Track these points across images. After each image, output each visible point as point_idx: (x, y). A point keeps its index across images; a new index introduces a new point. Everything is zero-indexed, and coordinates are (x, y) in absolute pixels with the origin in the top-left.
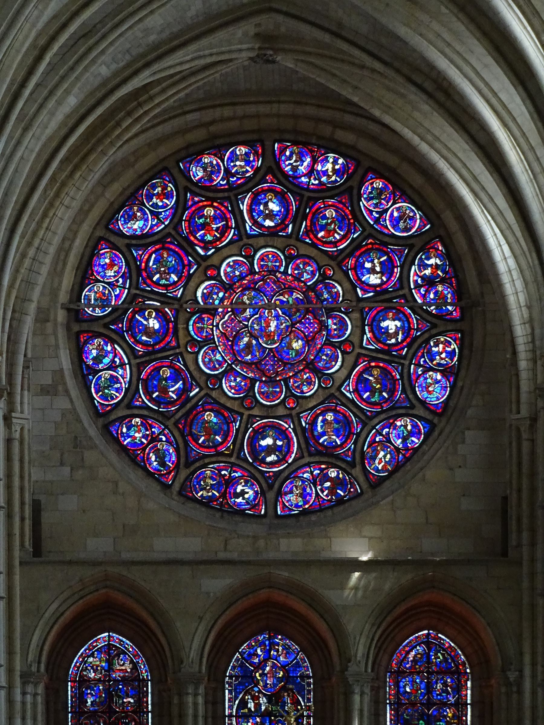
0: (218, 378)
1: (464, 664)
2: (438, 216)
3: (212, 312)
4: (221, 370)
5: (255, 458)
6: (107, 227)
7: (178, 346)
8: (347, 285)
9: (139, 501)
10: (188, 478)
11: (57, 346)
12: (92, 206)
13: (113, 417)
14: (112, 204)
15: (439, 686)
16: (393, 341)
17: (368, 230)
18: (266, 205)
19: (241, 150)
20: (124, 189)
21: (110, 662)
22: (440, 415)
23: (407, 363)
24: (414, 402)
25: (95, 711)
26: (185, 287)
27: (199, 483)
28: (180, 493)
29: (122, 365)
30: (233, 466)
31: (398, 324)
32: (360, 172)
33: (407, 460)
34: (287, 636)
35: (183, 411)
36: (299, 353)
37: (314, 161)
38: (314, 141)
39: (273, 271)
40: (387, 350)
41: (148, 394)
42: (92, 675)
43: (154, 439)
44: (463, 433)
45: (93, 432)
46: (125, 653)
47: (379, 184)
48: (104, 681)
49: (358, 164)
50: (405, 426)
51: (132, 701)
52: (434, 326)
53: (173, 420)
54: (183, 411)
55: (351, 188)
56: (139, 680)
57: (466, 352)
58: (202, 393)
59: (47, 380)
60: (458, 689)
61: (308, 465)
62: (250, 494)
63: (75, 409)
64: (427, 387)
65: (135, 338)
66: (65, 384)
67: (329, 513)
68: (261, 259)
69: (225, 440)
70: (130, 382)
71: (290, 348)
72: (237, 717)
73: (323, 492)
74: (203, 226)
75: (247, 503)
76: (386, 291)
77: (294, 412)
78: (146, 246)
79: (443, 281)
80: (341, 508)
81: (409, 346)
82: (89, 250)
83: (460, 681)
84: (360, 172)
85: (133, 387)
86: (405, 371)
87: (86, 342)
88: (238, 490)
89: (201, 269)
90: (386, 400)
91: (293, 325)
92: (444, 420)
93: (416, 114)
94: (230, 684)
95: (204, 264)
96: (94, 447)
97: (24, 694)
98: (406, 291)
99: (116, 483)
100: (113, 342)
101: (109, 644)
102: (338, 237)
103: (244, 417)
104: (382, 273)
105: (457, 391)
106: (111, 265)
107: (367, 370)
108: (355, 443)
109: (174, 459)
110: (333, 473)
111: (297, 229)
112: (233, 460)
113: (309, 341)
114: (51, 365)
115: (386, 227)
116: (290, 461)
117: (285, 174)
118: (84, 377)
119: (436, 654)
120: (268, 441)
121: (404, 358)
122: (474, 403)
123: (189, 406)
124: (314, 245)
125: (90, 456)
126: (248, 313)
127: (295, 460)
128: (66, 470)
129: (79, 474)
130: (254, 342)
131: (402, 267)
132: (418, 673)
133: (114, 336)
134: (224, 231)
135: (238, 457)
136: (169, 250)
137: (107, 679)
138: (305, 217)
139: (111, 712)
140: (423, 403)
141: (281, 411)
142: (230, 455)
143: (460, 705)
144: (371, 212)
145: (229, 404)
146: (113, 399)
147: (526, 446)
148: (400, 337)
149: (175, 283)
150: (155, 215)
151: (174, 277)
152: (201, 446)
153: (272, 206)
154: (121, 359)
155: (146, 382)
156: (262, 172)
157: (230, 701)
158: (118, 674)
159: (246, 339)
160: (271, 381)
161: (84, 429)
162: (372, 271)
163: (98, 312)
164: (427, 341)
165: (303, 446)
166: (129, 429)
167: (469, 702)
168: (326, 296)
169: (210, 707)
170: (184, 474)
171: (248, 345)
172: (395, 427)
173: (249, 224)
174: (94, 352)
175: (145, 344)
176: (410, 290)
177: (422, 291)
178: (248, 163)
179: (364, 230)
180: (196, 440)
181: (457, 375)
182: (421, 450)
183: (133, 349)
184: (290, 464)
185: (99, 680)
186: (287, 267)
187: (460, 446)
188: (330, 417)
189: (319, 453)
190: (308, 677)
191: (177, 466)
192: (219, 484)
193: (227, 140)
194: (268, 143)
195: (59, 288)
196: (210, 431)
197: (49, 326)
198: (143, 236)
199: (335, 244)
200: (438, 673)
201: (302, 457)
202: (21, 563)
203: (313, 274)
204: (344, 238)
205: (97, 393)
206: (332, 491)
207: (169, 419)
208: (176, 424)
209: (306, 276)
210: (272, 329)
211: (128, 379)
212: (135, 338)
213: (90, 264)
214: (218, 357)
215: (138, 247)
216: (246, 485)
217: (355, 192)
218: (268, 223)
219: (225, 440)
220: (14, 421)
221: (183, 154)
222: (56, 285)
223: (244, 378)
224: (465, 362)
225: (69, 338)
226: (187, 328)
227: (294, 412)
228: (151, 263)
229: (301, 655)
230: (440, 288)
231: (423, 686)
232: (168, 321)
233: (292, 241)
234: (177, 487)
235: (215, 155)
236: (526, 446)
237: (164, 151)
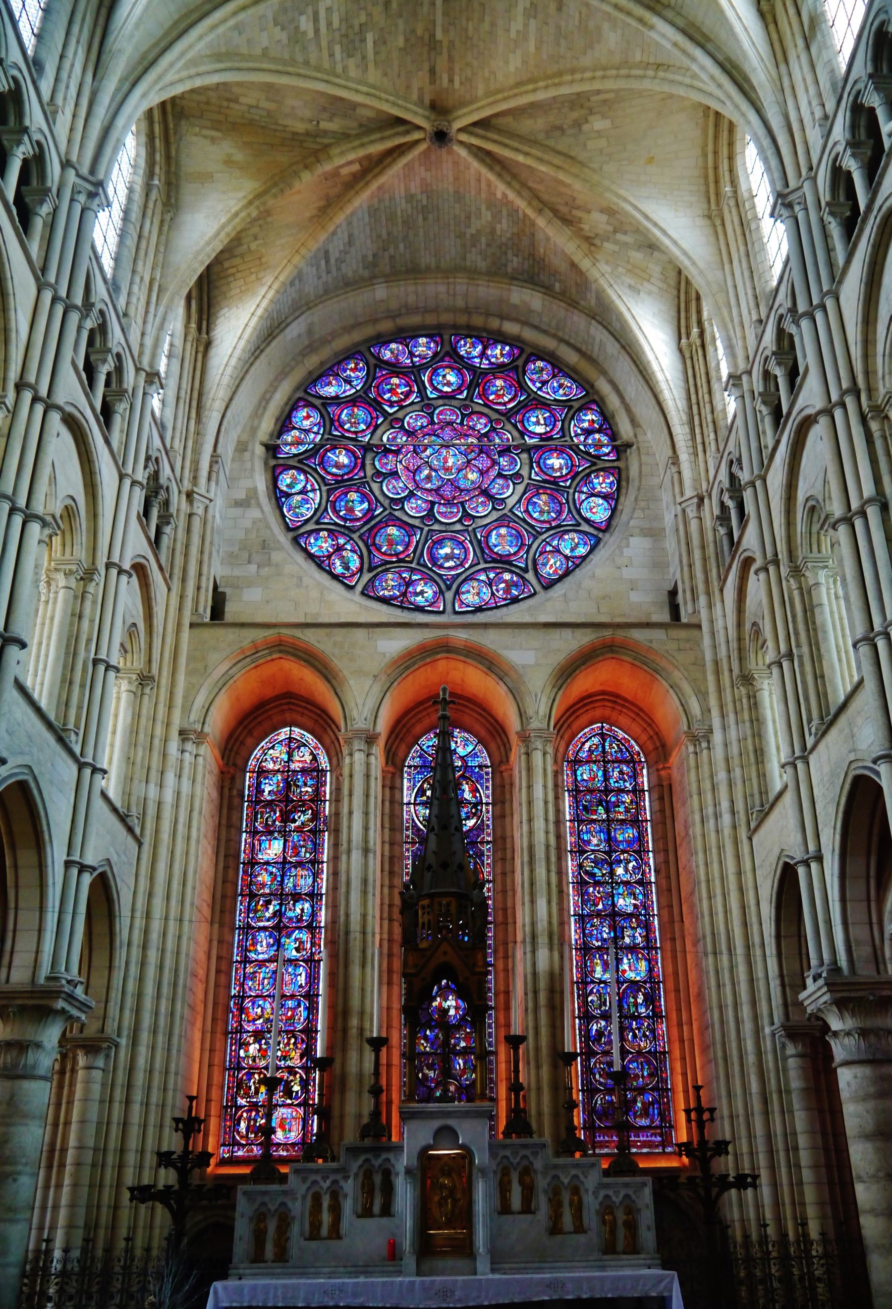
0: (401, 501)
1: (639, 754)
2: (592, 386)
3: (397, 453)
4: (403, 495)
5: (434, 564)
6: (306, 392)
7: (365, 477)
8: (516, 434)
9: (322, 593)
10: (371, 581)
11: (253, 469)
12: (292, 369)
13: (302, 530)
14: (310, 373)
15: (616, 774)
16: (558, 474)
17: (533, 395)
18: (444, 376)
19: (423, 340)
20: (322, 364)
21: (290, 754)
22: (604, 531)
23: (571, 491)
24: (581, 521)
25: (273, 801)
26: (372, 434)
27: (381, 582)
28: (363, 593)
29: (314, 490)
30: (413, 571)
31: (562, 461)
32: (524, 356)
33: (577, 566)
34: (464, 729)
35: (368, 526)
36: (473, 482)
37: (485, 348)
38: (485, 335)
39: (450, 423)
40: (555, 482)
41: (336, 512)
42: (271, 766)
43: (339, 549)
44: (627, 539)
45: (284, 539)
46: (305, 745)
47: (539, 364)
48: (283, 772)
49: (522, 351)
50: (573, 539)
51: (310, 790)
52: (594, 464)
53: (358, 534)
54: (368, 526)
55: (517, 366)
56: (318, 771)
57: (624, 483)
58: (386, 513)
59: (242, 495)
60: (635, 776)
61: (484, 570)
62: (429, 594)
63: (265, 519)
64: (591, 509)
65: (325, 470)
66: (257, 499)
67: (505, 609)
68: (441, 413)
69: (406, 549)
70: (320, 504)
71: (465, 477)
72: (415, 804)
73: (498, 591)
74: (390, 391)
75: (426, 601)
76: (551, 438)
77: (470, 529)
78: (338, 405)
79: (599, 431)
80: (516, 606)
81: (573, 479)
82: (288, 408)
83: (635, 769)
84: (524, 356)
85: (323, 507)
86: (570, 498)
87: (281, 473)
88: (418, 590)
89: (387, 421)
90: (554, 519)
91: (469, 461)
92: (607, 535)
93: (586, 170)
94: (409, 775)
95: (390, 418)
96: (280, 548)
97: (183, 751)
98: (568, 438)
99: (300, 579)
100: (305, 473)
101: (290, 738)
102: (506, 399)
103: (425, 532)
104: (546, 425)
105: (618, 513)
106: (308, 417)
107: (538, 494)
108: (527, 552)
109: (358, 564)
110: (507, 576)
111: (469, 397)
112: (413, 565)
113: (482, 473)
114: (245, 483)
115: (548, 393)
116: (467, 566)
117: (462, 357)
118: (278, 499)
119: (610, 745)
120: (446, 551)
121: (569, 487)
122: (636, 515)
123: (373, 523)
124: (485, 405)
125: (276, 556)
126: (428, 452)
127: (471, 566)
128: (253, 568)
129: (265, 571)
130: (434, 474)
131: (563, 421)
132: (595, 762)
133: (306, 468)
134: (407, 395)
135: (418, 564)
136: (358, 407)
137: (286, 771)
138: (478, 385)
139: (287, 800)
140: (587, 521)
141: (458, 527)
142: (411, 562)
143: (637, 791)
144: (534, 383)
145: (410, 521)
146: (302, 516)
147: (694, 525)
148: (564, 472)
149: (363, 431)
150: (348, 381)
151: (362, 427)
152: (384, 554)
153: (448, 377)
154: (312, 485)
155: (333, 504)
156: (441, 355)
157: (408, 789)
158: (297, 764)
159: (426, 472)
160: (449, 503)
161: (273, 534)
162: (538, 423)
163: (294, 451)
164: (589, 475)
165: (479, 554)
166: (316, 540)
167: (646, 788)
168: (497, 441)
169: (387, 791)
170: (367, 577)
171: (428, 478)
172: (564, 540)
173: (429, 389)
174: (288, 481)
175: (333, 475)
176: (571, 438)
177: (582, 438)
178: (430, 348)
179: (529, 395)
180: (379, 549)
181: (617, 501)
182: (588, 560)
183: (323, 478)
184: (466, 570)
185: (278, 771)
186: (462, 421)
187: (625, 550)
188: (503, 531)
189: (494, 561)
190: (487, 767)
191: (361, 570)
192: (400, 585)
193: (411, 334)
194: (446, 337)
195: (258, 427)
196: (391, 543)
197: (247, 455)
198: (337, 397)
199: (505, 404)
200: (613, 762)
201: (479, 564)
202: (192, 625)
203: (486, 426)
204: (510, 401)
205: (289, 511)
206: (507, 591)
207: (354, 532)
208: (360, 537)
209: (479, 427)
210: (450, 464)
211: (317, 501)
212: (325, 470)
213: (289, 417)
214: (401, 485)
215: (330, 405)
216: (426, 584)
217: (520, 370)
218: (446, 389)
219: (406, 549)
220: (195, 496)
221: (374, 342)
222: (256, 423)
223: (426, 501)
224: (623, 491)
225: (266, 471)
226: (374, 464)
227: (470, 529)
228: (343, 416)
229: (480, 747)
230: (597, 436)
231: (600, 773)
232: (356, 458)
233: (467, 402)
234: (359, 588)
235: (401, 343)
236: (694, 525)
237: (357, 336)
